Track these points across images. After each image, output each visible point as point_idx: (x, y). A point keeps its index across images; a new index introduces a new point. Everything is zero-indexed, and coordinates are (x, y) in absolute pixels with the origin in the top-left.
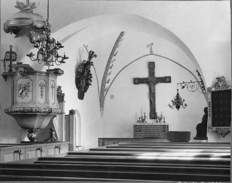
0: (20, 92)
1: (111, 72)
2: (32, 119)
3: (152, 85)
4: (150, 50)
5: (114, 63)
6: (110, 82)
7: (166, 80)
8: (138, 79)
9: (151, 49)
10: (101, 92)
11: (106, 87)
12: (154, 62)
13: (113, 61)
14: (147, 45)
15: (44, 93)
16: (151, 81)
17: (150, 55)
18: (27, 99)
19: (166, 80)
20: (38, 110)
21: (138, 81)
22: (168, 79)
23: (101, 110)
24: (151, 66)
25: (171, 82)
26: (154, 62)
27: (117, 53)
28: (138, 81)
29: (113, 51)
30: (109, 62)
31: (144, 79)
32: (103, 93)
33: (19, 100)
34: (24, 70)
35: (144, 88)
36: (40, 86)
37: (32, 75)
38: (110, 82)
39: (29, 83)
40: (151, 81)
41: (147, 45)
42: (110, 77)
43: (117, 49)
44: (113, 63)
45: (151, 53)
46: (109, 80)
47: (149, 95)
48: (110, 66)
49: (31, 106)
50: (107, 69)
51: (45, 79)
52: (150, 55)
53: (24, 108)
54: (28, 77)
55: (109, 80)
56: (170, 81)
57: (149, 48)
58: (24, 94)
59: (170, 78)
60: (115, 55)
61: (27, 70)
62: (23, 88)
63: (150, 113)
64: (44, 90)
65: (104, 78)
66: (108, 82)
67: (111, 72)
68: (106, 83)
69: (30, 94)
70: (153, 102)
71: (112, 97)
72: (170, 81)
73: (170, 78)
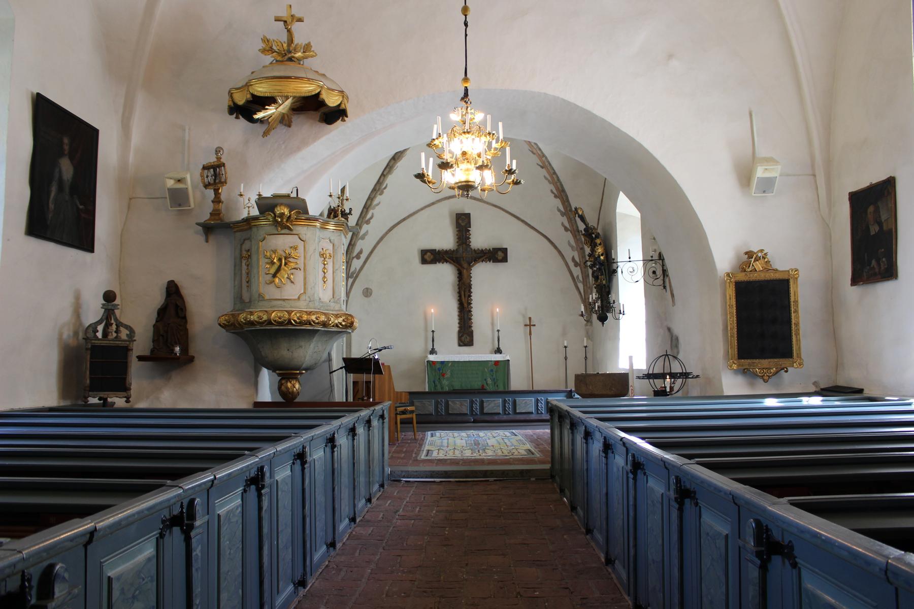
0: (273, 271)
2: (302, 343)
3: (465, 265)
6: (363, 257)
7: (497, 255)
12: (469, 215)
13: (374, 208)
15: (329, 275)
16: (463, 257)
18: (291, 291)
19: (497, 255)
20: (305, 317)
21: (431, 257)
24: (462, 223)
26: (469, 215)
28: (431, 257)
31: (446, 252)
33: (270, 292)
34: (290, 212)
35: (446, 272)
36: (322, 255)
37: (305, 228)
38: (363, 257)
39: (295, 248)
46: (361, 252)
48: (369, 216)
49: (302, 305)
51: (332, 238)
53: (289, 313)
54: (294, 232)
55: (361, 252)
56: (505, 259)
58: (284, 274)
59: (505, 251)
61: (298, 213)
62: (280, 260)
63: (459, 332)
64: (330, 267)
66: (358, 257)
69: (299, 276)
70: (466, 305)
72: (505, 259)
73: (505, 251)
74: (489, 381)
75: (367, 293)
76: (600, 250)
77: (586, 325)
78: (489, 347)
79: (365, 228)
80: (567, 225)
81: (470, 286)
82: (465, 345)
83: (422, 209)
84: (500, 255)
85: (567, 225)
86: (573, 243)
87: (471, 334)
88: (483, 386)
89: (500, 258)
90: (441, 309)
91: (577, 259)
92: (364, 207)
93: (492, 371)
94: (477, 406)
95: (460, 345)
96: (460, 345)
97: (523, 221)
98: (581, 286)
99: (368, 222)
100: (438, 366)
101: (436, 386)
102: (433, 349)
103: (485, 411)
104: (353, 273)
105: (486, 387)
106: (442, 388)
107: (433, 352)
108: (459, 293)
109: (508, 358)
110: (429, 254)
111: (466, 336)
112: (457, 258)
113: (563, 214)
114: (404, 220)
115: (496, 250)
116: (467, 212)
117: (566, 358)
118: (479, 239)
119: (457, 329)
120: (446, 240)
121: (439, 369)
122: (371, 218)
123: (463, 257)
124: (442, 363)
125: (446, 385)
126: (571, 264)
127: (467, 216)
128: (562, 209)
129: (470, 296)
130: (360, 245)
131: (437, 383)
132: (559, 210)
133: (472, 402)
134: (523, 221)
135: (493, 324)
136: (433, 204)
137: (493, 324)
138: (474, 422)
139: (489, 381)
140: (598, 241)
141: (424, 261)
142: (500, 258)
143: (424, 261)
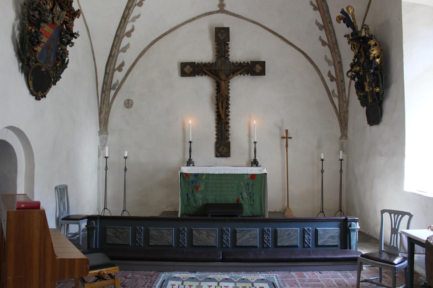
1: (128, 45)
3: (223, 77)
5: (136, 24)
6: (125, 69)
7: (255, 68)
8: (192, 64)
10: (103, 91)
11: (114, 81)
12: (228, 29)
17: (217, 12)
19: (255, 68)
21: (190, 69)
23: (100, 133)
24: (221, 37)
25: (265, 75)
26: (228, 29)
28: (190, 69)
30: (125, 18)
32: (107, 91)
35: (205, 85)
38: (125, 69)
40: (221, 70)
42: (126, 58)
44: (135, 24)
45: (222, 9)
46: (123, 64)
47: (216, 102)
50: (118, 38)
52: (217, 12)
55: (123, 64)
56: (262, 73)
59: (262, 64)
63: (217, 143)
65: (112, 57)
67: (128, 45)
68: (114, 70)
70: (223, 117)
71: (128, 104)
72: (262, 73)
73: (262, 64)
74: (245, 195)
75: (128, 104)
76: (374, 52)
77: (341, 138)
78: (245, 159)
79: (125, 41)
80: (325, 39)
81: (228, 98)
82: (222, 156)
83: (183, 24)
84: (258, 68)
85: (325, 39)
86: (330, 58)
87: (228, 146)
88: (238, 200)
89: (258, 71)
90: (199, 120)
91: (333, 74)
92: (123, 17)
93: (248, 184)
94: (228, 238)
95: (217, 156)
96: (217, 156)
97: (280, 37)
98: (336, 101)
99: (129, 34)
100: (192, 178)
101: (189, 199)
102: (190, 159)
103: (238, 243)
104: (115, 85)
105: (241, 201)
106: (196, 202)
107: (190, 163)
108: (217, 105)
109: (265, 171)
110: (188, 67)
111: (223, 148)
112: (215, 71)
113: (321, 28)
114: (165, 34)
115: (254, 63)
116: (226, 26)
117: (322, 171)
118: (238, 53)
119: (215, 140)
120: (205, 54)
121: (193, 182)
122: (132, 30)
123: (221, 70)
124: (196, 175)
125: (200, 198)
126: (327, 79)
127: (227, 30)
128: (321, 22)
129: (228, 108)
130: (121, 58)
131: (190, 196)
132: (317, 24)
133: (222, 232)
134: (280, 37)
135: (250, 136)
136: (193, 19)
137: (250, 136)
138: (223, 260)
139: (245, 195)
140: (372, 42)
141: (183, 74)
142: (258, 71)
143: (183, 74)
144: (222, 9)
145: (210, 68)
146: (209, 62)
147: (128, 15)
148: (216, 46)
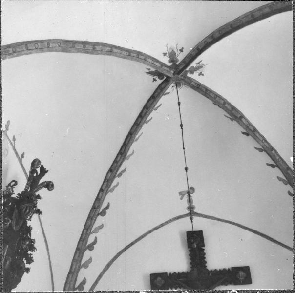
1: (91, 259)
4: (187, 205)
5: (100, 235)
8: (163, 275)
9: (190, 201)
13: (96, 231)
14: (180, 193)
22: (241, 273)
24: (195, 242)
26: (201, 232)
27: (107, 208)
29: (99, 200)
41: (180, 193)
43: (109, 198)
44: (97, 235)
45: (192, 213)
57: (186, 197)
59: (246, 270)
60: (103, 213)
67: (91, 259)
73: (246, 270)
79: (87, 254)
99: (91, 247)
114: (132, 244)
118: (216, 261)
122: (95, 242)
144: (192, 213)
145: (185, 279)
146: (183, 272)
147: (91, 226)
148: (189, 253)
